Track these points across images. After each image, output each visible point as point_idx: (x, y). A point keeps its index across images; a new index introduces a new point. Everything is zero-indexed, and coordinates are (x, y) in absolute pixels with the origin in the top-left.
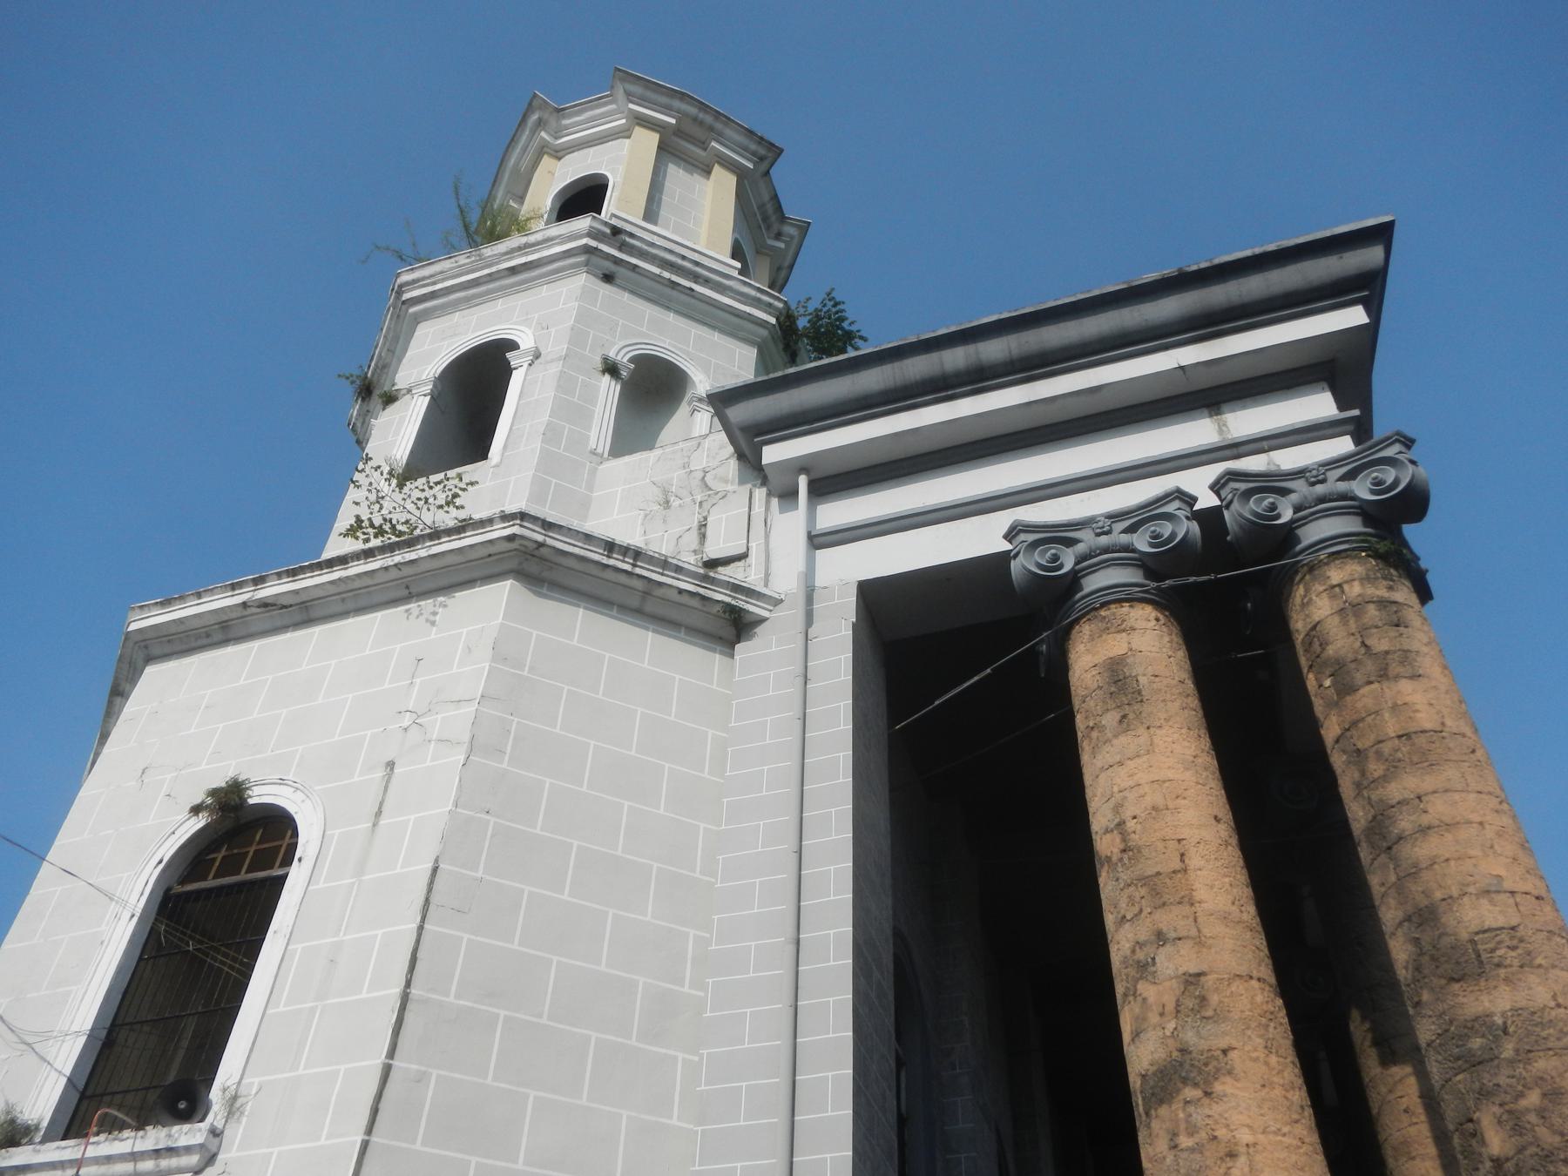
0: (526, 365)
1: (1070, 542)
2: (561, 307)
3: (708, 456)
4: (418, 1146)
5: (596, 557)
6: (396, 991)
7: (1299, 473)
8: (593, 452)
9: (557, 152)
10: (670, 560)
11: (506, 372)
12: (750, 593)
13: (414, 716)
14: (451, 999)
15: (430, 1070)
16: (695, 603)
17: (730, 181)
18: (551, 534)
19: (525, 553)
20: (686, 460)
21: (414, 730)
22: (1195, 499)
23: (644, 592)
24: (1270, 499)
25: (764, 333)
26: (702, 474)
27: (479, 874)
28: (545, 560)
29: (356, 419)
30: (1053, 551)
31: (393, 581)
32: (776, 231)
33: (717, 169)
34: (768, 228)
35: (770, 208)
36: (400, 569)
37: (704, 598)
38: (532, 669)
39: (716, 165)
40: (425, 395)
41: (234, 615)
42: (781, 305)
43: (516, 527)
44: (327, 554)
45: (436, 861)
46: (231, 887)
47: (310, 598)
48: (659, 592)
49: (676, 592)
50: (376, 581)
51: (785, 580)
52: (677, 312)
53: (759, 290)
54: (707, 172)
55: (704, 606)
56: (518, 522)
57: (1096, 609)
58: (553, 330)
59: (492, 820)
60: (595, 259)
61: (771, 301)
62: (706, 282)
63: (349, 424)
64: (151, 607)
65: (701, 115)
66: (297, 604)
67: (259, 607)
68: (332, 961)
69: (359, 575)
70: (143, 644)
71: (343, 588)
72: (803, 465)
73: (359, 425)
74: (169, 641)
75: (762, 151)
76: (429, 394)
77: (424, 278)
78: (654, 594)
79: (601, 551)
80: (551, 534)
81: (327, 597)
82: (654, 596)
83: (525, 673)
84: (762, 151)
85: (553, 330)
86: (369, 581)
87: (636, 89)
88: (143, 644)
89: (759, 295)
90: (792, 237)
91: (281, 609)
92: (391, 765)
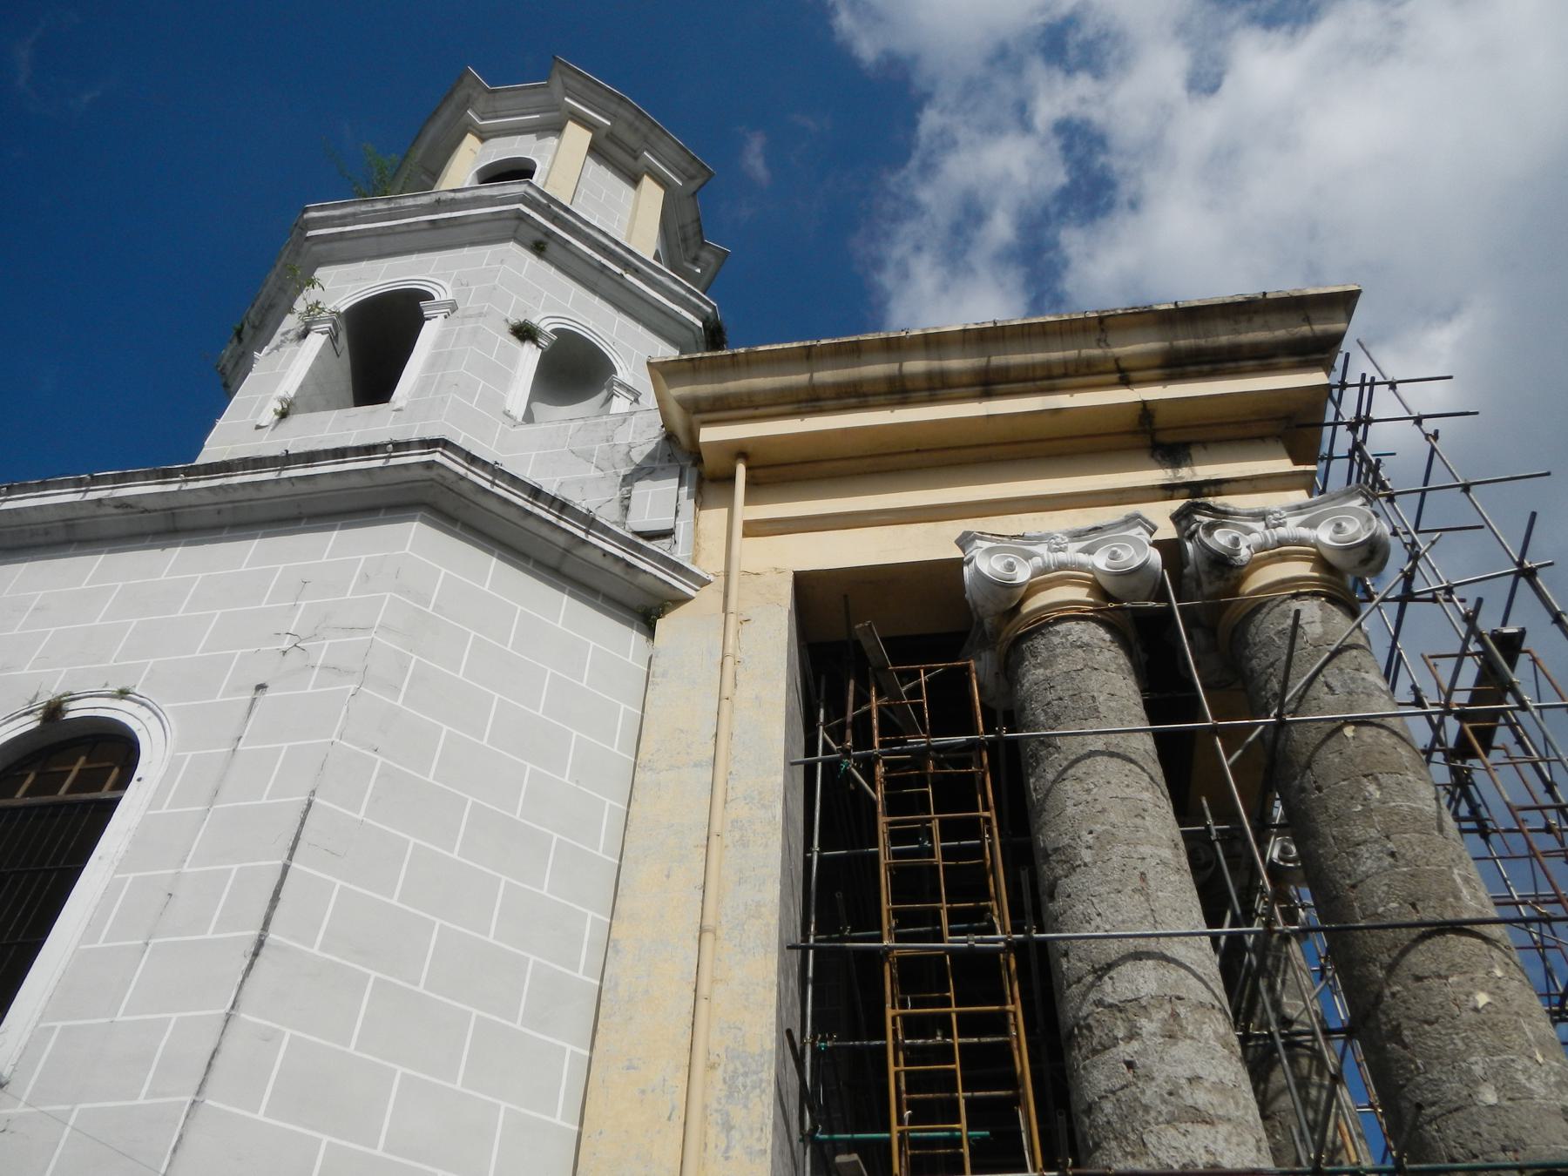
0: (441, 317)
1: (1029, 556)
2: (484, 267)
3: (634, 432)
4: (260, 1116)
5: (520, 502)
6: (254, 933)
7: (1261, 516)
8: (507, 414)
9: (481, 132)
10: (598, 518)
11: (418, 321)
12: (677, 568)
13: (296, 639)
14: (315, 950)
15: (283, 1029)
16: (618, 569)
17: (659, 193)
18: (473, 468)
19: (442, 485)
20: (610, 433)
21: (295, 653)
22: (1155, 529)
23: (564, 549)
24: (1236, 533)
25: (689, 335)
26: (628, 449)
27: (360, 816)
28: (465, 498)
29: (228, 361)
30: (1011, 560)
32: (693, 255)
33: (647, 182)
34: (686, 250)
35: (691, 230)
36: (293, 484)
37: (629, 565)
38: (437, 608)
39: (645, 176)
40: (322, 333)
41: (83, 513)
42: (709, 310)
43: (438, 454)
44: (201, 460)
45: (313, 793)
46: (43, 807)
47: (177, 505)
48: (583, 552)
49: (599, 553)
50: (262, 495)
51: (709, 565)
52: (603, 297)
53: (688, 290)
54: (634, 181)
55: (627, 573)
56: (440, 449)
57: (1052, 625)
58: (474, 288)
59: (380, 759)
60: (524, 228)
61: (701, 304)
62: (636, 272)
63: (217, 366)
65: (637, 123)
66: (164, 510)
67: (116, 507)
68: (170, 895)
69: (243, 485)
71: (221, 498)
72: (741, 451)
73: (229, 367)
75: (692, 170)
76: (327, 332)
78: (574, 552)
79: (526, 497)
80: (473, 468)
82: (575, 555)
83: (430, 610)
84: (692, 170)
85: (474, 288)
86: (252, 493)
87: (571, 82)
89: (688, 295)
90: (709, 264)
91: (142, 512)
92: (261, 687)
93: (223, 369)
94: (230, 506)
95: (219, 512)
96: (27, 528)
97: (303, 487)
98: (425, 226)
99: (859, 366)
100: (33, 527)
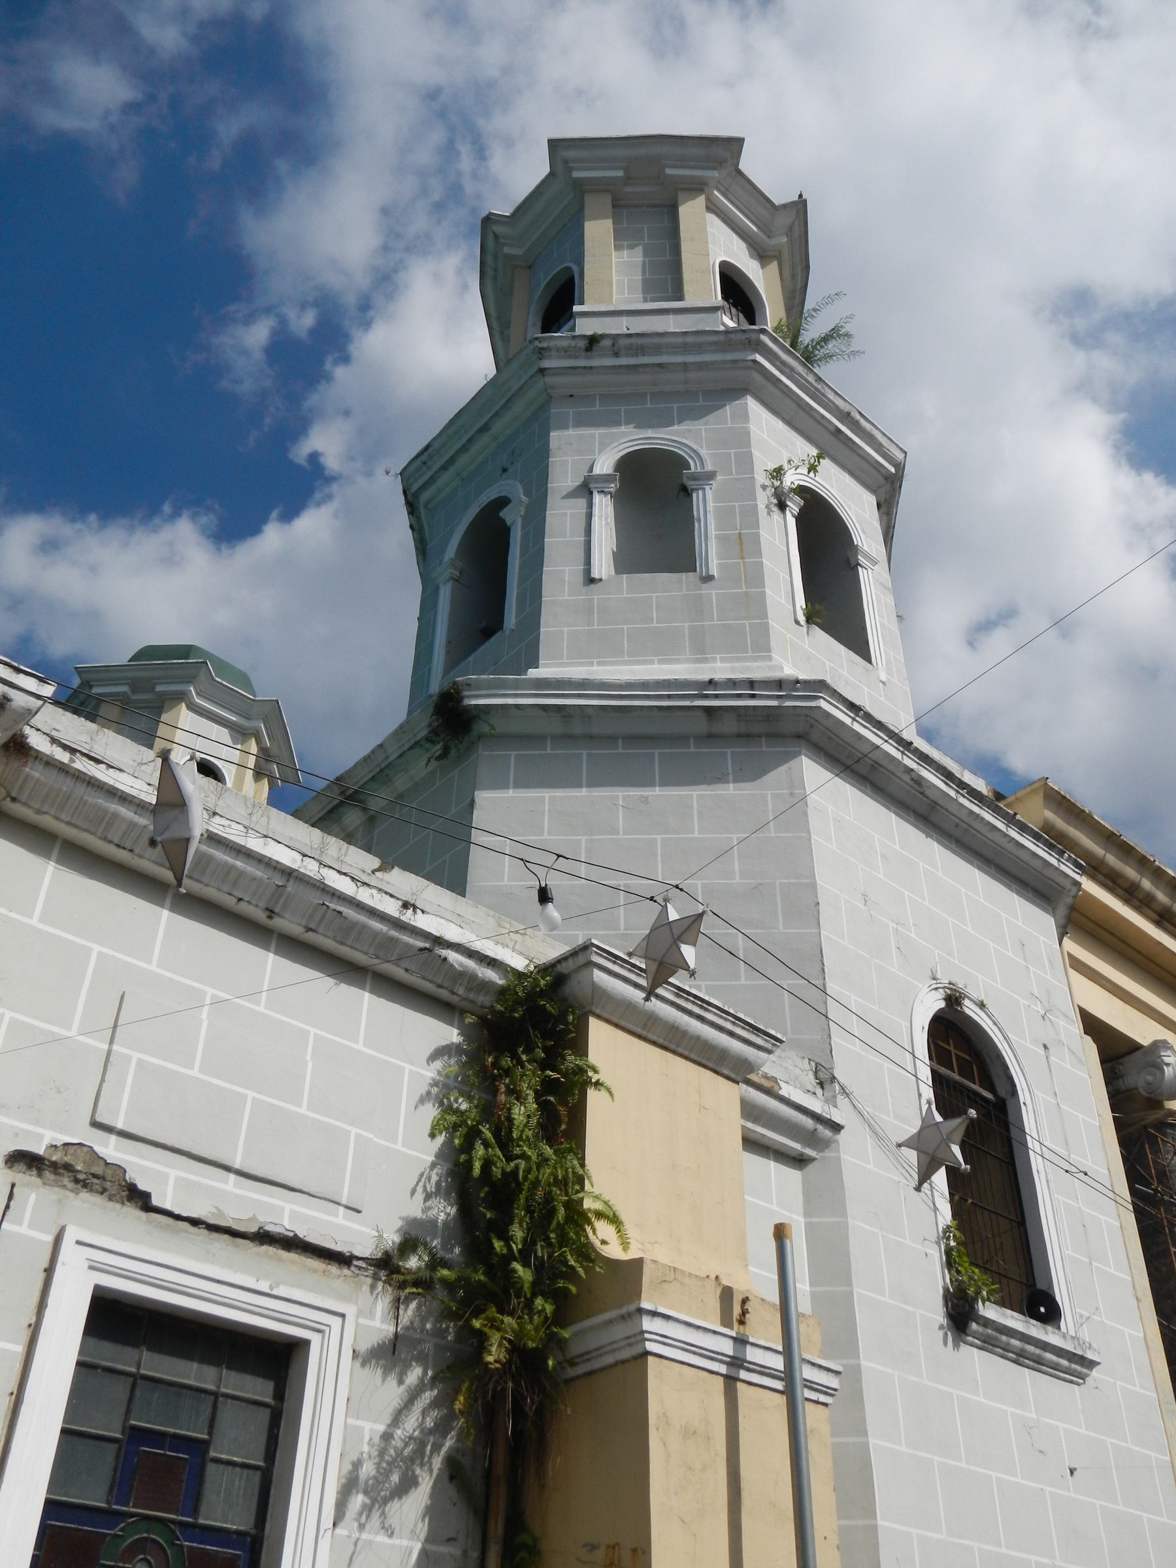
31: (993, 841)
41: (890, 767)
47: (943, 805)
64: (841, 700)
65: (798, 293)
66: (932, 801)
67: (912, 779)
69: (989, 823)
70: (813, 721)
74: (830, 738)
77: (778, 357)
81: (951, 813)
86: (984, 830)
87: (796, 229)
88: (813, 721)
91: (921, 793)
93: (542, 348)
94: (965, 826)
95: (957, 825)
96: (850, 748)
97: (1010, 847)
98: (832, 429)
99: (1125, 863)
100: (854, 750)
